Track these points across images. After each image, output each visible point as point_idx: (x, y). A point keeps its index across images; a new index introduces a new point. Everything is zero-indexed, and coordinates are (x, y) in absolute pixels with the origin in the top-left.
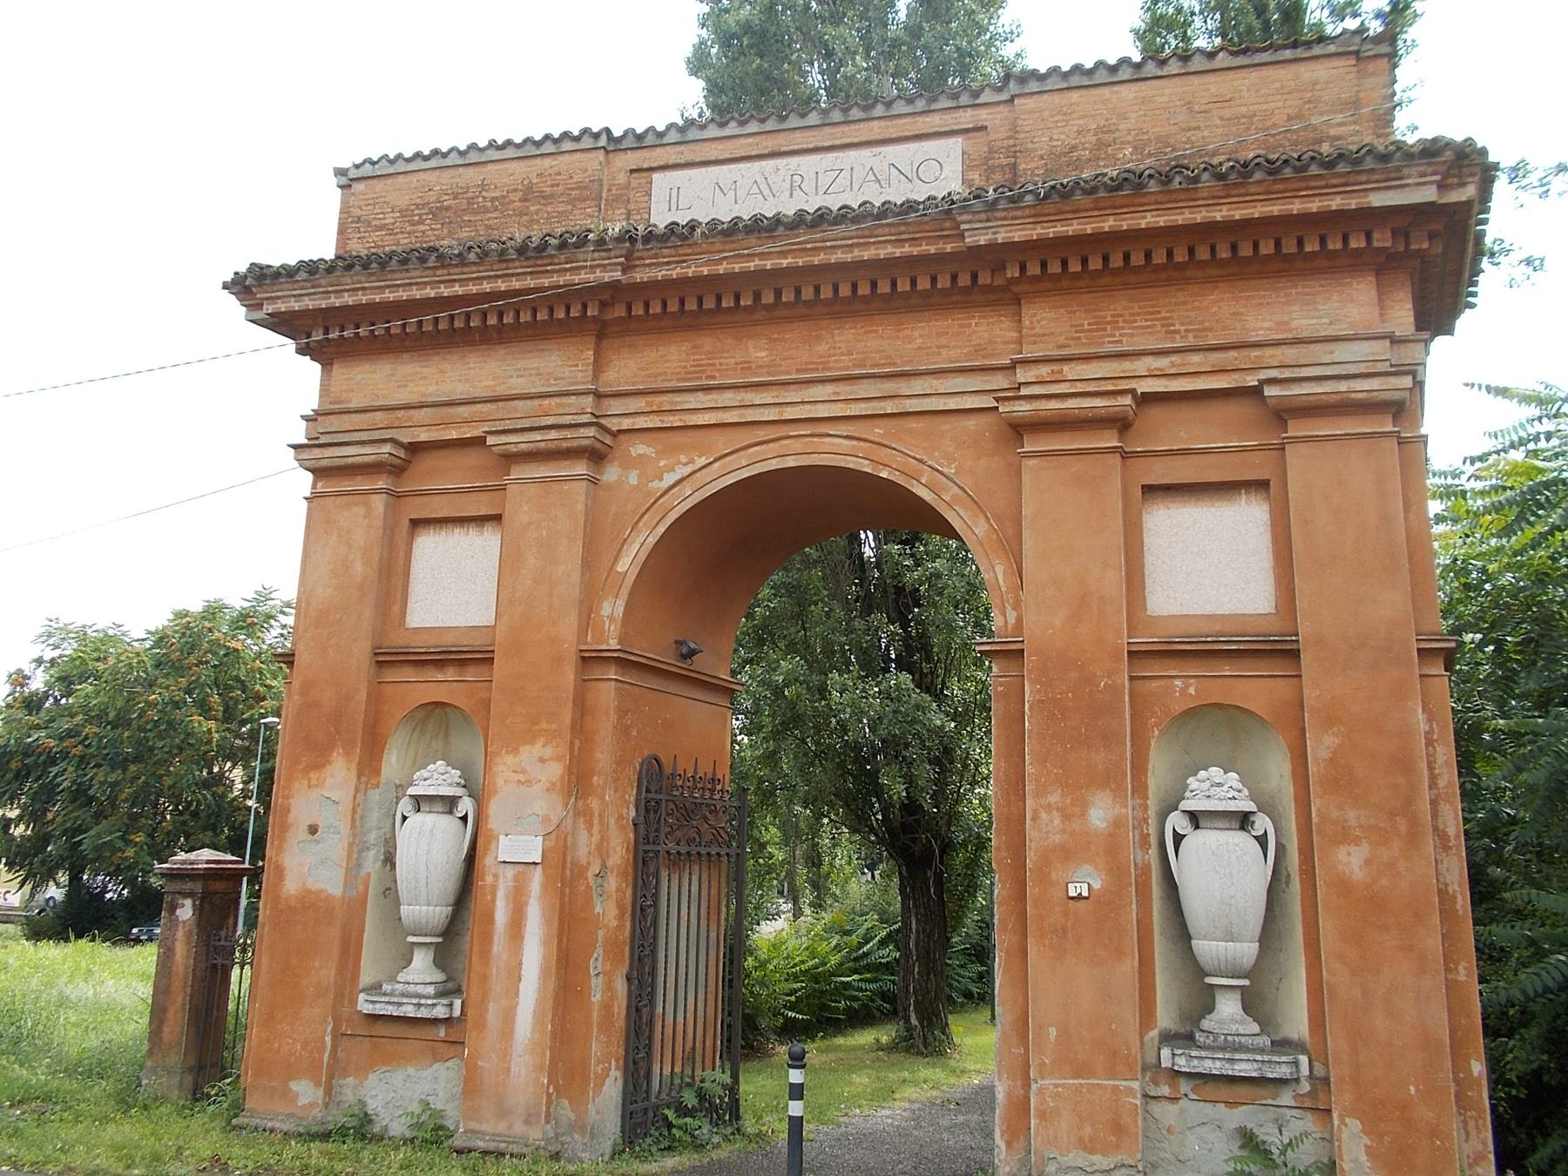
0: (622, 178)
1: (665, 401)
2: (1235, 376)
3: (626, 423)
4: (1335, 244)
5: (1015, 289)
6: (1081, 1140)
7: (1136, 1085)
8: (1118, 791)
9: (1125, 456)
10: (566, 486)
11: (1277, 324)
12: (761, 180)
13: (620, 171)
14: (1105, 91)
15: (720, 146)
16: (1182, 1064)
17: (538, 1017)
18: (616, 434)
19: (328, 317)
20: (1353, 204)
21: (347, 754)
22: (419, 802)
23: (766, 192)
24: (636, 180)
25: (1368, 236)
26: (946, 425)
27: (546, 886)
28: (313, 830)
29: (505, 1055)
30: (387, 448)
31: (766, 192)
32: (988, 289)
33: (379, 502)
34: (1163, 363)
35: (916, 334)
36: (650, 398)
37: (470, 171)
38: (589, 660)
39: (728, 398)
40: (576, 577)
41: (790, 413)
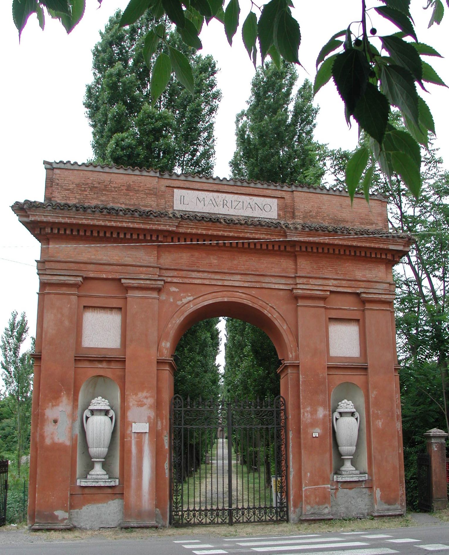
0: (163, 188)
1: (184, 273)
2: (353, 289)
3: (169, 280)
4: (379, 256)
5: (297, 253)
6: (316, 502)
7: (329, 486)
8: (325, 407)
9: (326, 308)
10: (150, 301)
11: (363, 275)
12: (213, 199)
13: (162, 185)
14: (319, 195)
15: (199, 184)
16: (340, 479)
17: (150, 483)
18: (165, 282)
19: (52, 225)
20: (385, 247)
21: (68, 394)
22: (93, 412)
23: (215, 204)
24: (167, 190)
25: (386, 255)
26: (274, 292)
27: (150, 440)
28: (55, 421)
29: (139, 496)
30: (80, 279)
31: (215, 204)
32: (289, 252)
33: (74, 299)
34: (335, 282)
35: (265, 262)
36: (178, 272)
37: (105, 175)
38: (160, 362)
39: (205, 275)
40: (155, 334)
41: (226, 283)
